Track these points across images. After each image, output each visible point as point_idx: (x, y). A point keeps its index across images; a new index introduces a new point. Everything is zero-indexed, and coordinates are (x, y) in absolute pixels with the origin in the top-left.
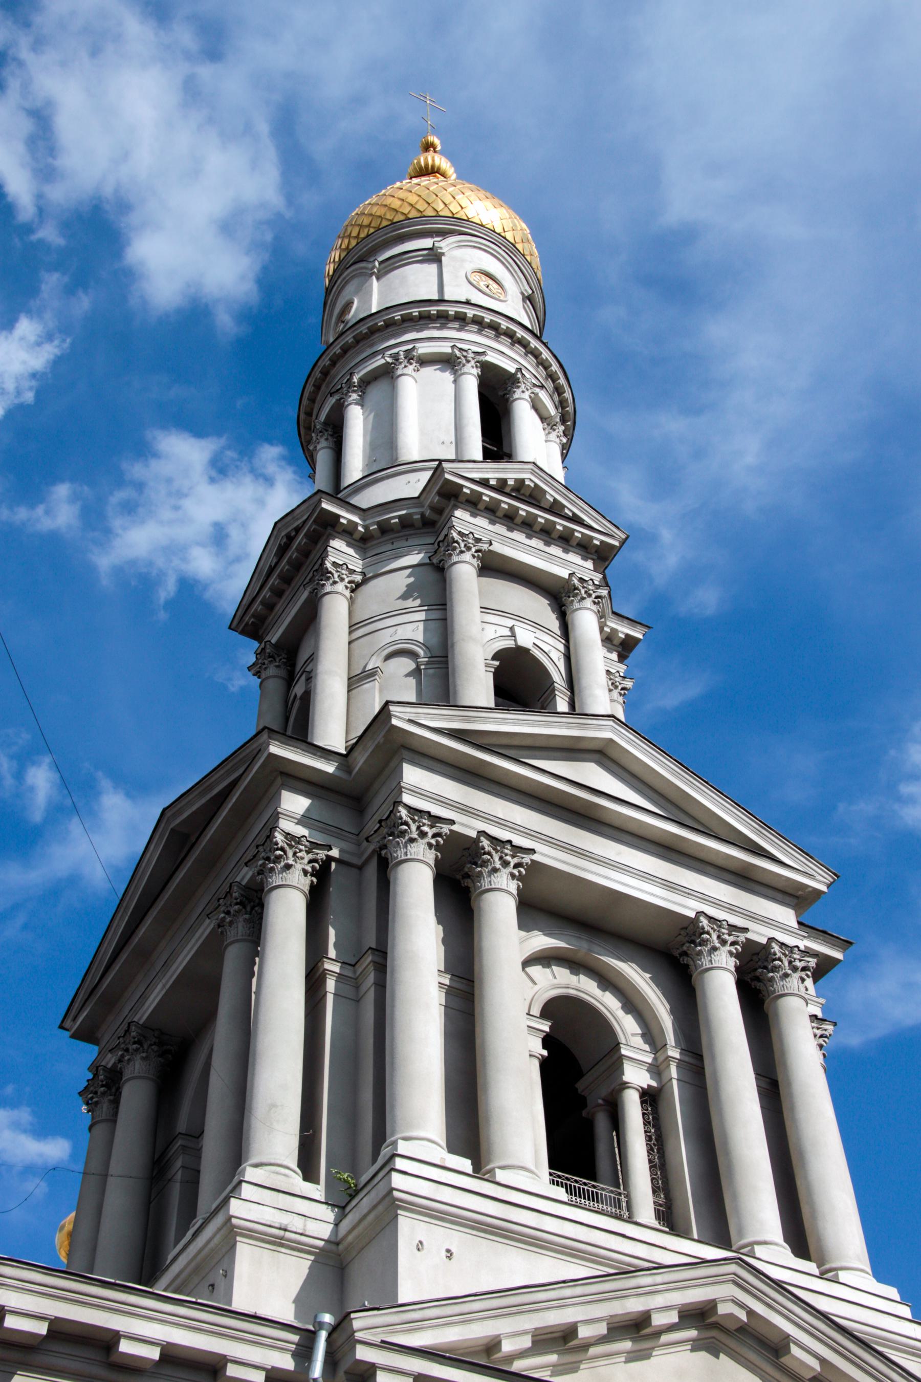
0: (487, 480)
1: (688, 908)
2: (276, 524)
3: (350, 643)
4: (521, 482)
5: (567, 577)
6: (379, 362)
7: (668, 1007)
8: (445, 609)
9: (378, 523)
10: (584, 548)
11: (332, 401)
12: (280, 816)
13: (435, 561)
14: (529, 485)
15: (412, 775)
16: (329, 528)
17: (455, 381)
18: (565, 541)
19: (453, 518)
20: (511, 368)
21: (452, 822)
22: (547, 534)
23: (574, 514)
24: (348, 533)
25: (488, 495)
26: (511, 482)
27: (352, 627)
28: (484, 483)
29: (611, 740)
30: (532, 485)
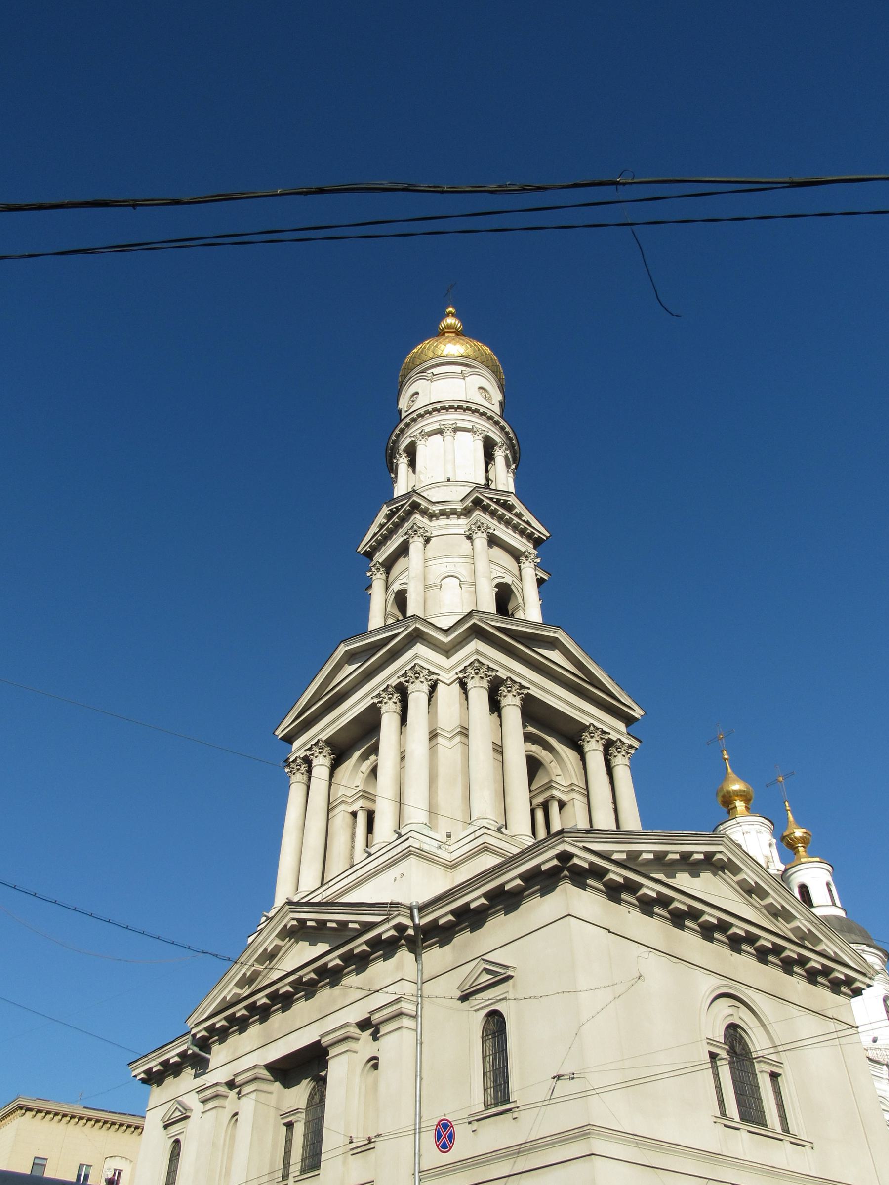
0: (493, 498)
1: (587, 721)
4: (506, 501)
6: (436, 426)
8: (473, 559)
11: (408, 441)
13: (467, 533)
14: (509, 504)
17: (474, 441)
20: (498, 440)
21: (498, 671)
22: (515, 528)
23: (528, 521)
25: (494, 506)
28: (491, 499)
29: (557, 638)
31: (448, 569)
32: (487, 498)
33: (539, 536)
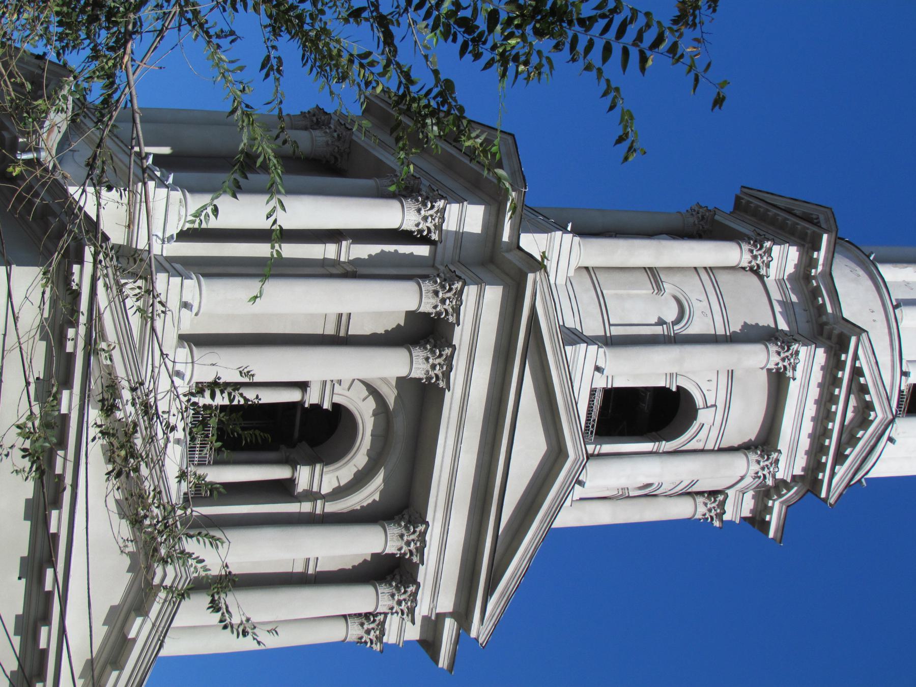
0: (863, 375)
1: (434, 514)
2: (831, 209)
3: (695, 268)
5: (778, 449)
7: (365, 504)
9: (818, 287)
10: (815, 466)
12: (461, 204)
14: (870, 415)
15: (494, 295)
16: (810, 245)
18: (817, 449)
19: (813, 346)
24: (807, 263)
25: (845, 375)
26: (867, 398)
27: (709, 270)
28: (857, 372)
29: (567, 456)
30: (871, 418)
31: (696, 305)
32: (856, 357)
33: (822, 481)
